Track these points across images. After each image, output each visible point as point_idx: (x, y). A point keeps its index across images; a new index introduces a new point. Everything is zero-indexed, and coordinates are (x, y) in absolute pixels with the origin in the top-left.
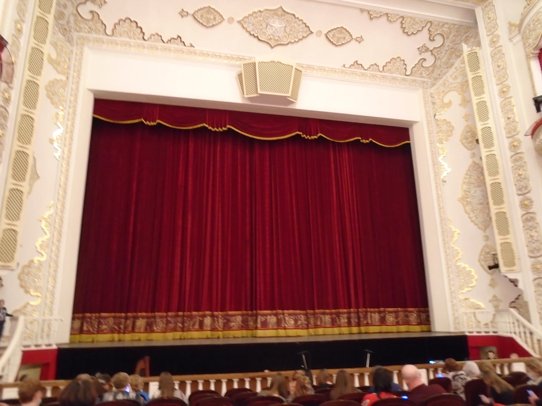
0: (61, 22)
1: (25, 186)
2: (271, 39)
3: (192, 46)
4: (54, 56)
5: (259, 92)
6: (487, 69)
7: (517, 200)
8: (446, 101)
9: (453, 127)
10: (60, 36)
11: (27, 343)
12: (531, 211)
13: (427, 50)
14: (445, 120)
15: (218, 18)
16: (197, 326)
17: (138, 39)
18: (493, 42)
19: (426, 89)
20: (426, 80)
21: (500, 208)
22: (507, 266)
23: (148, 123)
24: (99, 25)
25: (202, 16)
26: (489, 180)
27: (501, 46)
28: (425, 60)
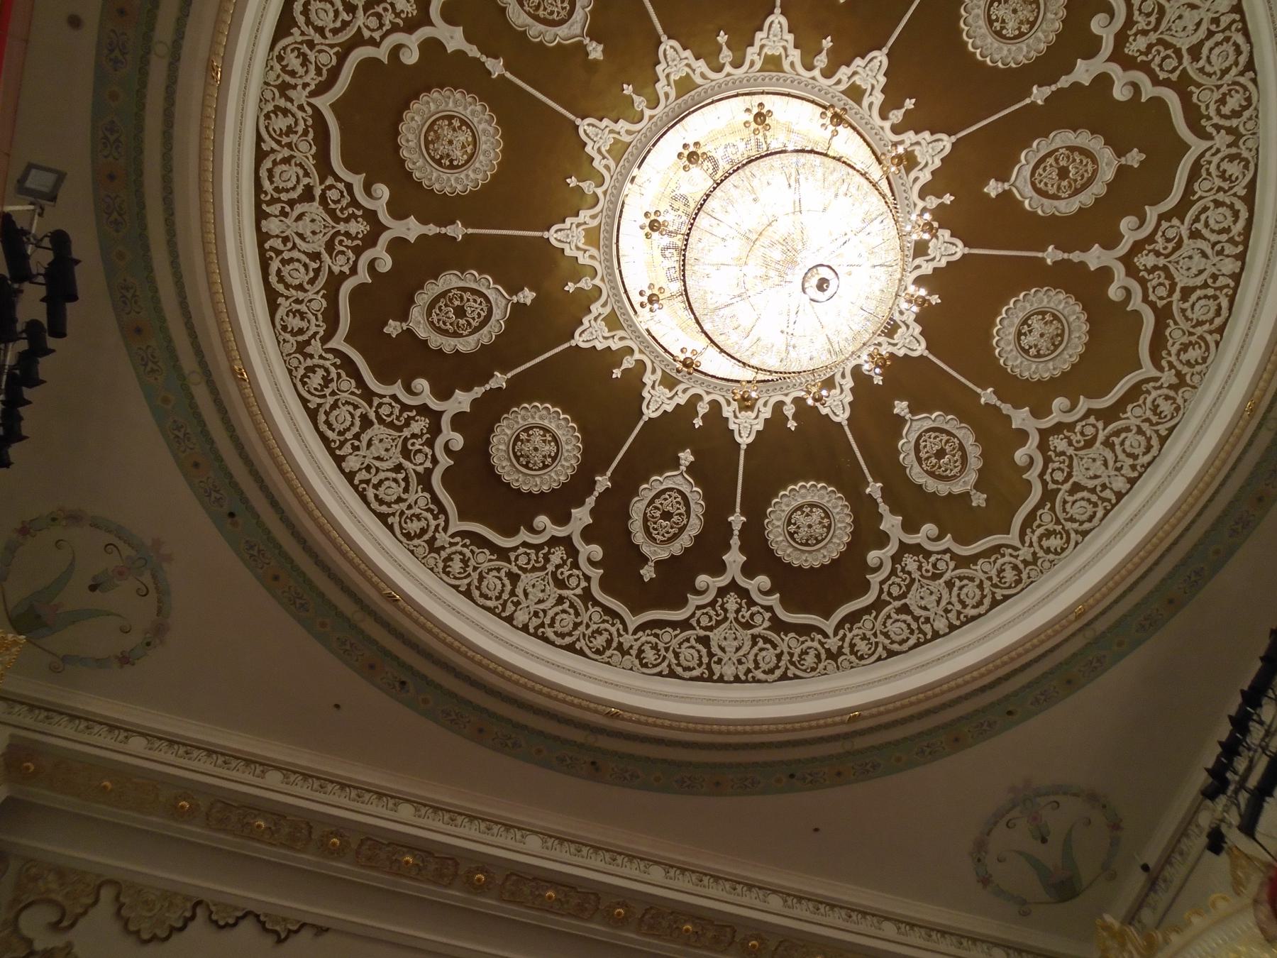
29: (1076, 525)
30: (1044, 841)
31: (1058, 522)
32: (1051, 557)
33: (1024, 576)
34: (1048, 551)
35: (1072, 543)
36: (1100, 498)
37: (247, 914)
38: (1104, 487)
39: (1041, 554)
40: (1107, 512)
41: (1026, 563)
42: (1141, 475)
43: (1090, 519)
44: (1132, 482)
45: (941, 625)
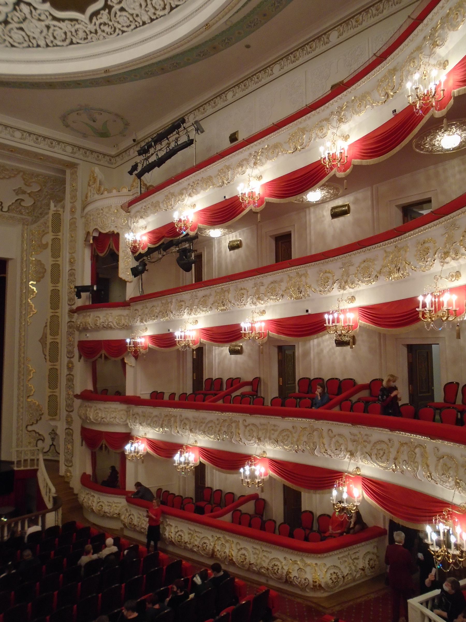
6: (65, 234)
7: (65, 360)
8: (44, 242)
9: (45, 269)
12: (72, 373)
13: (24, 192)
14: (40, 261)
18: (73, 212)
19: (27, 225)
20: (26, 217)
21: (54, 365)
22: (51, 416)
26: (49, 339)
27: (75, 218)
28: (22, 200)
29: (119, 26)
30: (94, 121)
31: (111, 20)
32: (104, 34)
33: (89, 37)
34: (103, 31)
35: (116, 33)
36: (134, 19)
38: (137, 16)
39: (99, 31)
40: (136, 27)
41: (91, 32)
42: (157, 18)
43: (128, 27)
44: (152, 20)
45: (42, 43)
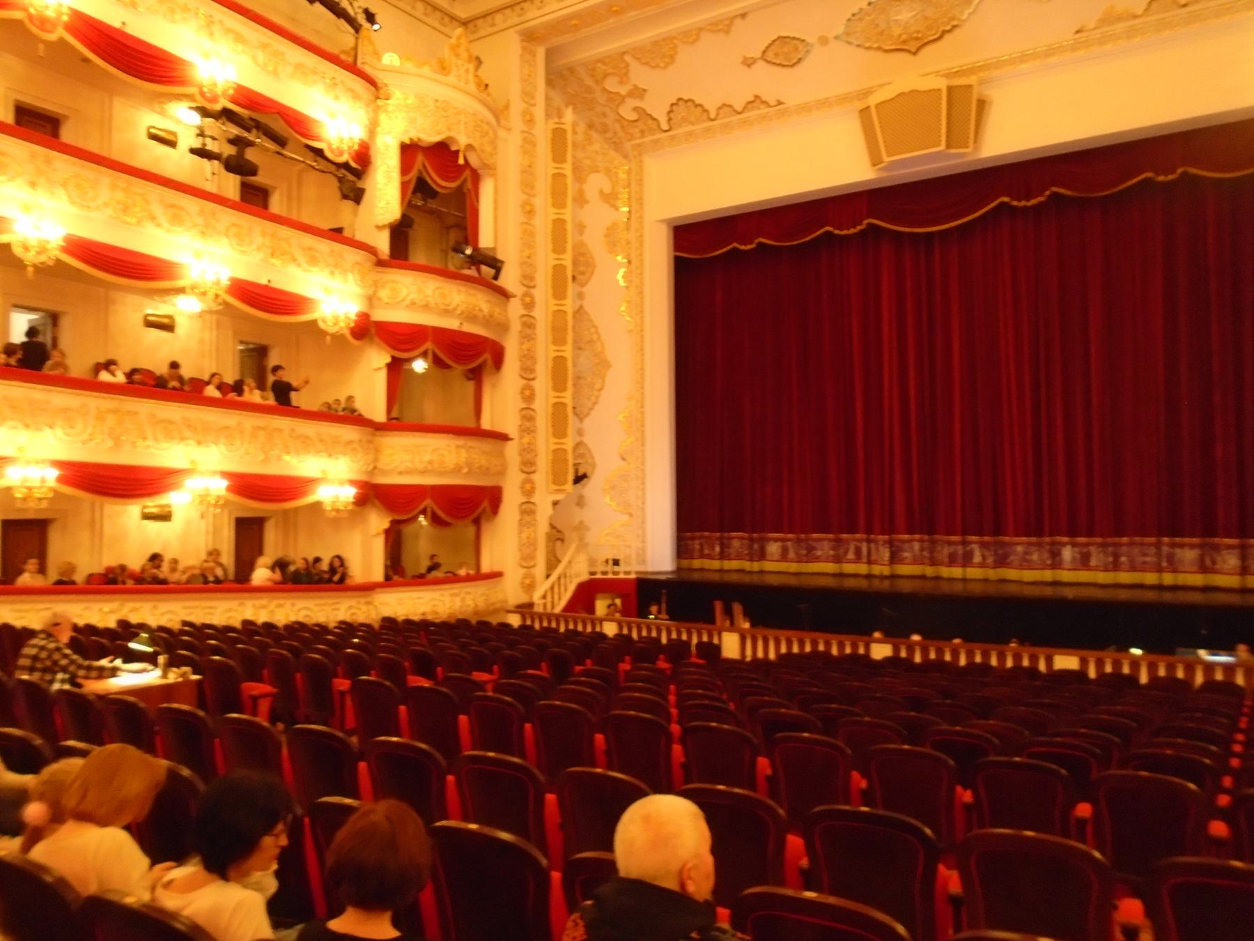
0: (609, 135)
1: (567, 397)
2: (904, 42)
3: (780, 103)
4: (607, 190)
5: (887, 159)
10: (612, 153)
11: (593, 570)
15: (801, 47)
16: (851, 556)
17: (704, 121)
23: (743, 247)
24: (650, 122)
25: (776, 55)
37: (700, 30)
